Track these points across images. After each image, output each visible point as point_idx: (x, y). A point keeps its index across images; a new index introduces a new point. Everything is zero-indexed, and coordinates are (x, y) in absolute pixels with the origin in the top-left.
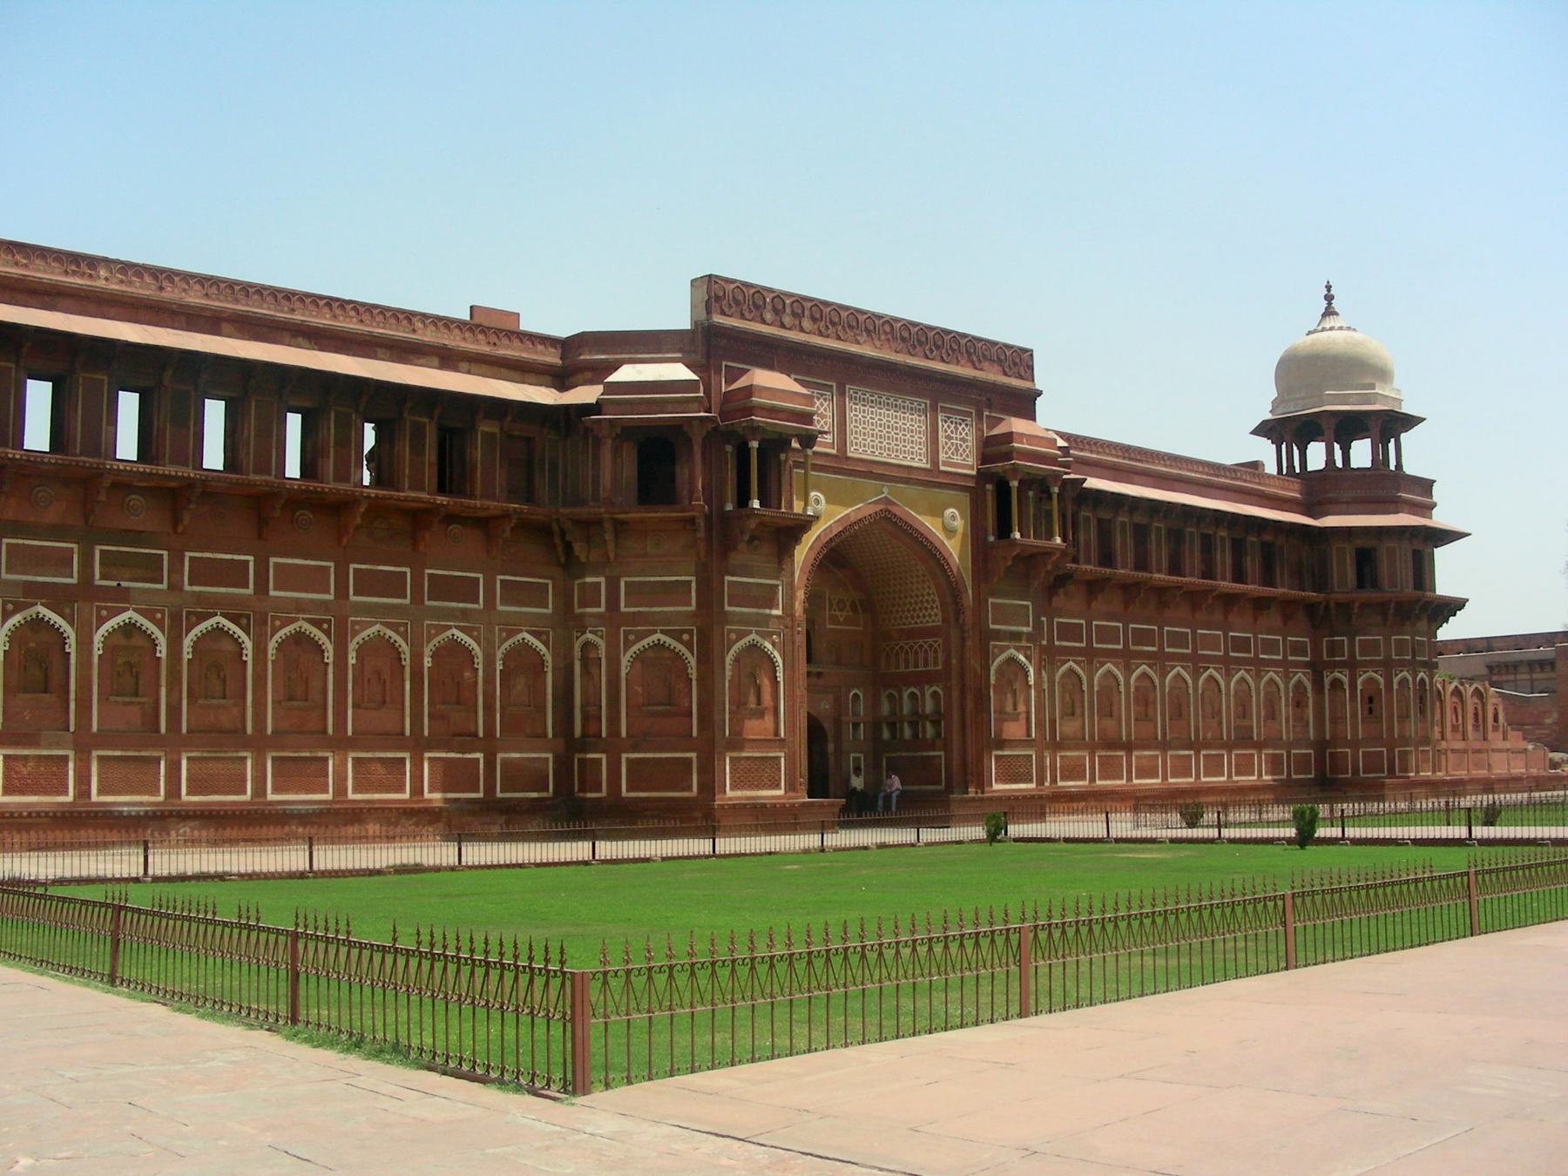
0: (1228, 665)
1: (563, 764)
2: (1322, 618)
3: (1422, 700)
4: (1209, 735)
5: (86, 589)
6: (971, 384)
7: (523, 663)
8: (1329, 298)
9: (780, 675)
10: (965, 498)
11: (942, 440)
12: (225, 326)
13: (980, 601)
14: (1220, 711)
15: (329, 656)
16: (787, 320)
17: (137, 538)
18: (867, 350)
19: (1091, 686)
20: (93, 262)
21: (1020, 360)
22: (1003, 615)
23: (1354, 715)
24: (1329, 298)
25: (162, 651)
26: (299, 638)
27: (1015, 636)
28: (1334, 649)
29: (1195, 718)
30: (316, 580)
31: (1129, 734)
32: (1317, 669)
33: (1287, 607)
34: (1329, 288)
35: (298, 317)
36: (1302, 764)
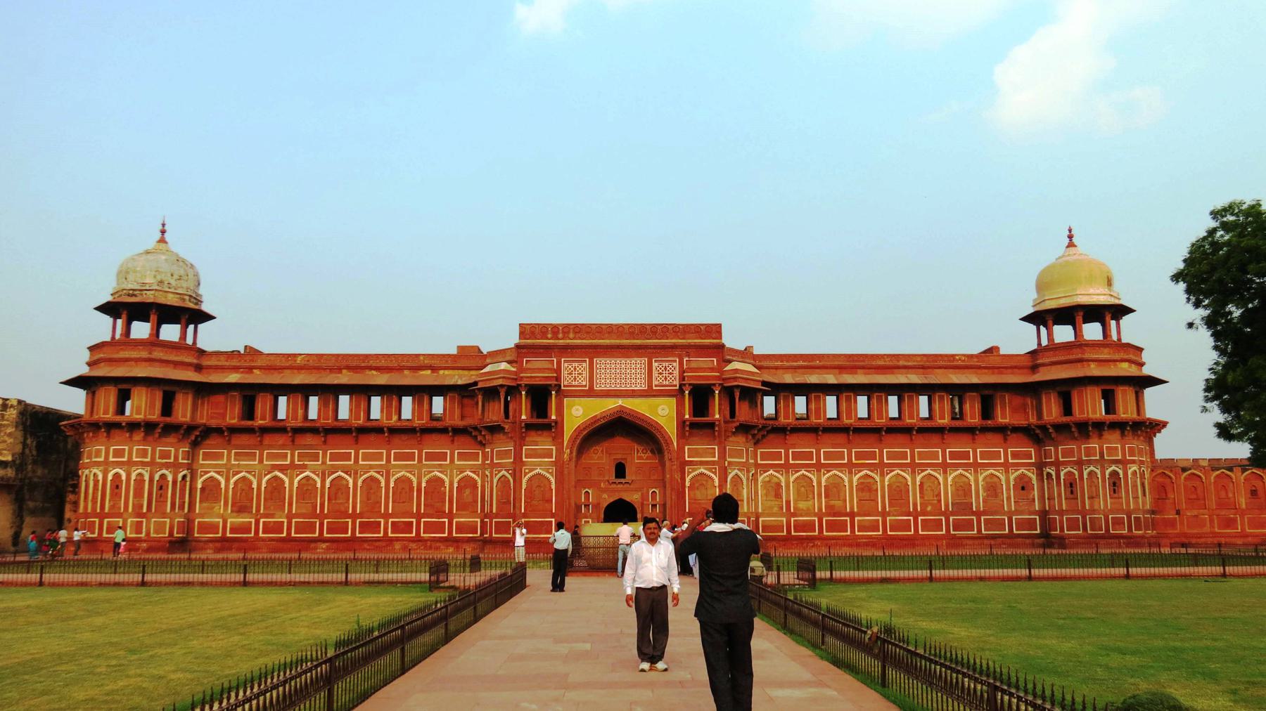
0: (944, 467)
1: (482, 521)
2: (1037, 435)
3: (1114, 484)
4: (929, 508)
5: (292, 466)
6: (674, 347)
7: (467, 484)
8: (1070, 237)
9: (553, 487)
10: (673, 401)
11: (655, 374)
12: (344, 371)
13: (681, 449)
14: (939, 495)
15: (383, 484)
16: (560, 336)
17: (311, 447)
18: (607, 342)
19: (819, 483)
20: (295, 355)
21: (715, 330)
22: (693, 453)
23: (1060, 495)
24: (1070, 237)
25: (319, 485)
26: (372, 478)
27: (702, 463)
28: (1047, 454)
29: (914, 498)
30: (378, 457)
31: (852, 507)
32: (1040, 466)
33: (1002, 430)
34: (1070, 231)
35: (372, 363)
36: (1030, 524)
